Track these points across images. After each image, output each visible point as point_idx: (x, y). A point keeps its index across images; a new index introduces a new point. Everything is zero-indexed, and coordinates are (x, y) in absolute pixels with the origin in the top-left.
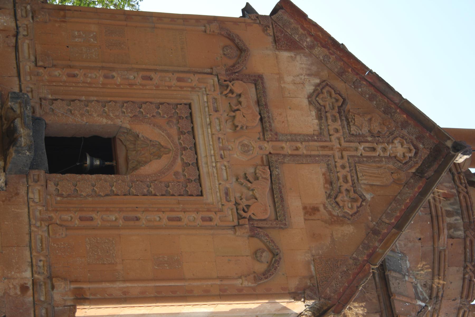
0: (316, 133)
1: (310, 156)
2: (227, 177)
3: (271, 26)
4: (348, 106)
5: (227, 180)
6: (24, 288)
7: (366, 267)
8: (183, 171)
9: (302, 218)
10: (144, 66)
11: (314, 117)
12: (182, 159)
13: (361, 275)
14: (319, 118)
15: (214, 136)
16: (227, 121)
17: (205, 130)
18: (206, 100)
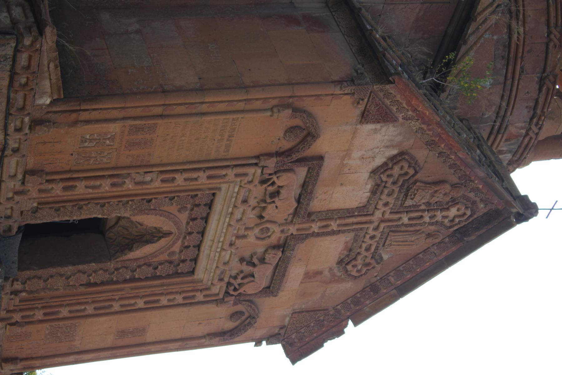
0: (361, 205)
1: (339, 231)
2: (229, 259)
3: (366, 100)
4: (418, 176)
5: (228, 262)
7: (344, 323)
8: (181, 251)
9: (299, 282)
10: (169, 168)
11: (368, 190)
12: (183, 243)
13: (334, 329)
14: (373, 192)
15: (230, 229)
16: (254, 208)
17: (222, 218)
18: (236, 190)
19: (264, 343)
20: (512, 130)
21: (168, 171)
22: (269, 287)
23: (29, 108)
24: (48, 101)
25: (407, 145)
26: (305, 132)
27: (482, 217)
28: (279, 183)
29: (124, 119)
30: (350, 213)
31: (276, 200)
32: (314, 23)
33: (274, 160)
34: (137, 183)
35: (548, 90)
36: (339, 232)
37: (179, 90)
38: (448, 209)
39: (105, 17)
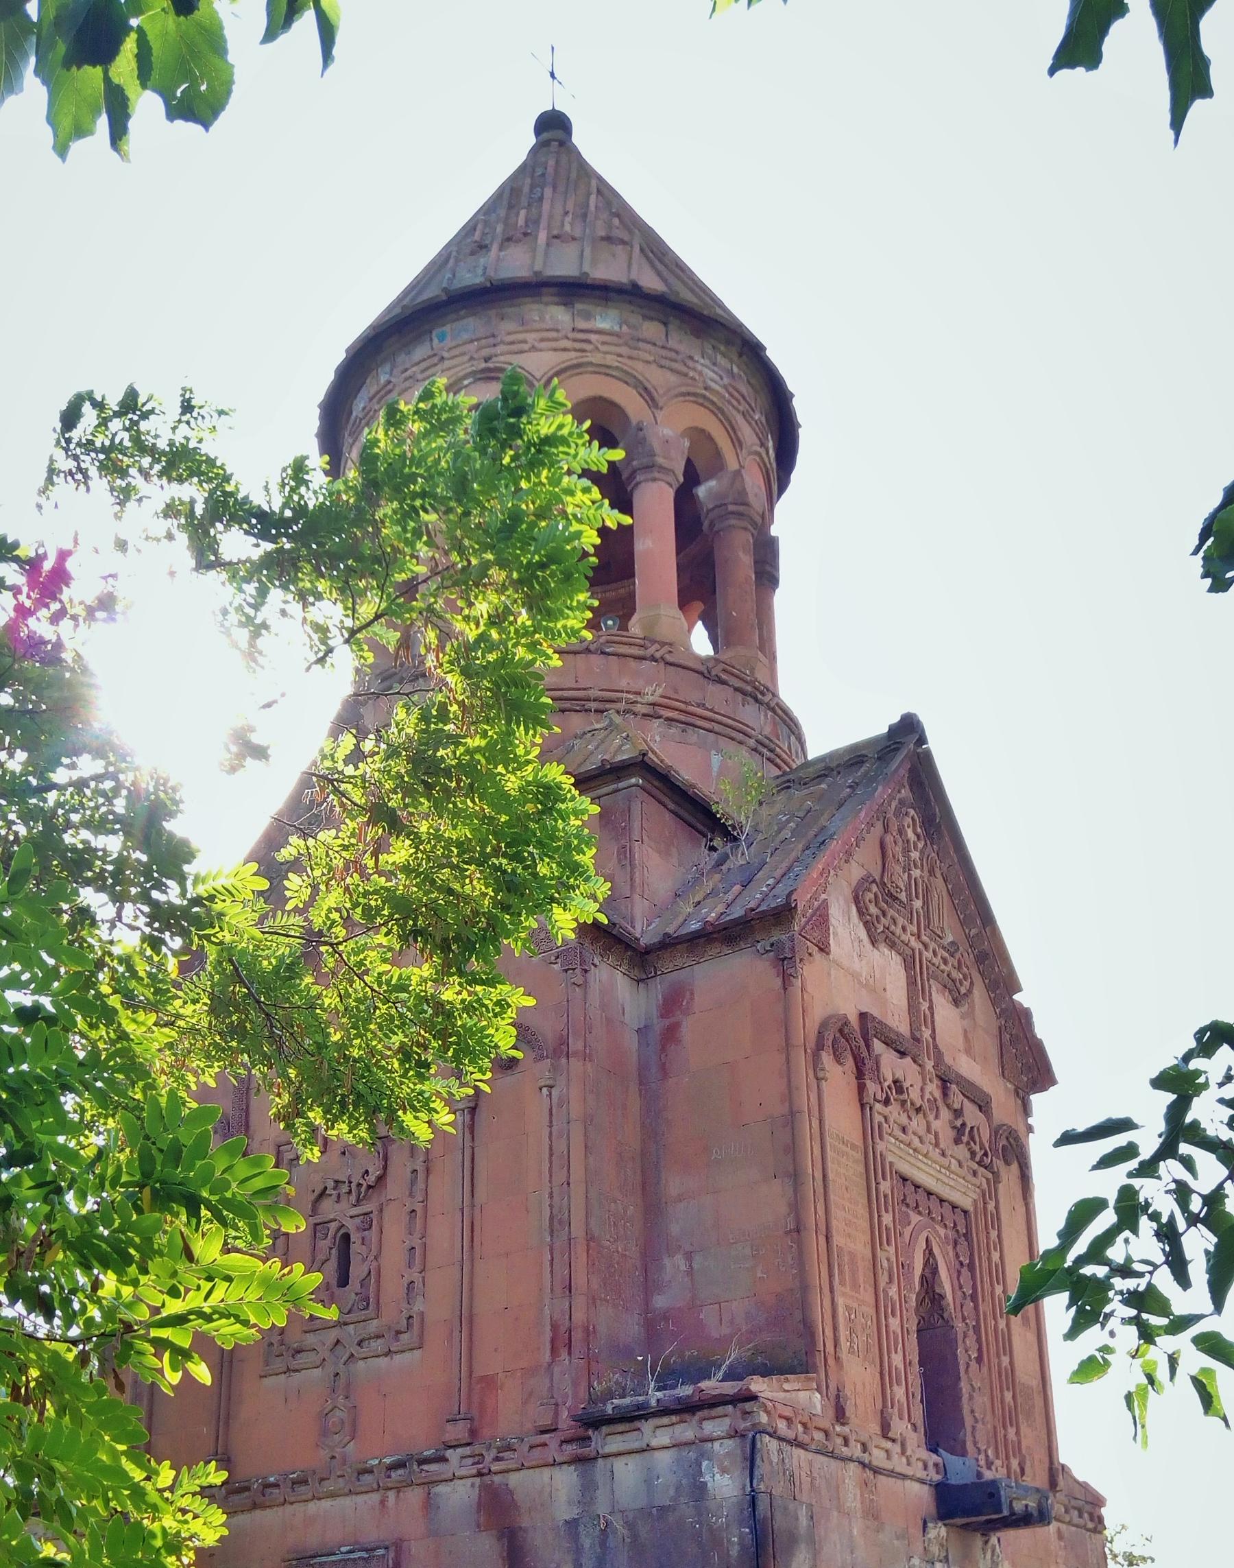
6: (1060, 1536)
14: (892, 946)
15: (930, 1154)
18: (893, 1140)
19: (1030, 1121)
20: (767, 730)
21: (878, 1237)
22: (980, 1108)
23: (825, 1424)
24: (818, 1396)
25: (848, 892)
26: (838, 1035)
27: (914, 794)
28: (889, 1082)
29: (832, 1291)
30: (911, 982)
31: (906, 1085)
32: (673, 1003)
33: (869, 1083)
34: (891, 1281)
35: (725, 670)
36: (931, 1000)
37: (796, 1207)
38: (908, 841)
39: (660, 1302)
